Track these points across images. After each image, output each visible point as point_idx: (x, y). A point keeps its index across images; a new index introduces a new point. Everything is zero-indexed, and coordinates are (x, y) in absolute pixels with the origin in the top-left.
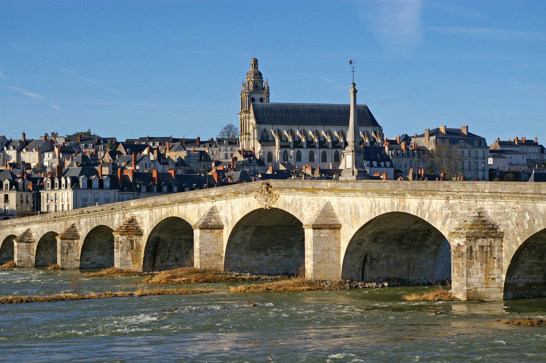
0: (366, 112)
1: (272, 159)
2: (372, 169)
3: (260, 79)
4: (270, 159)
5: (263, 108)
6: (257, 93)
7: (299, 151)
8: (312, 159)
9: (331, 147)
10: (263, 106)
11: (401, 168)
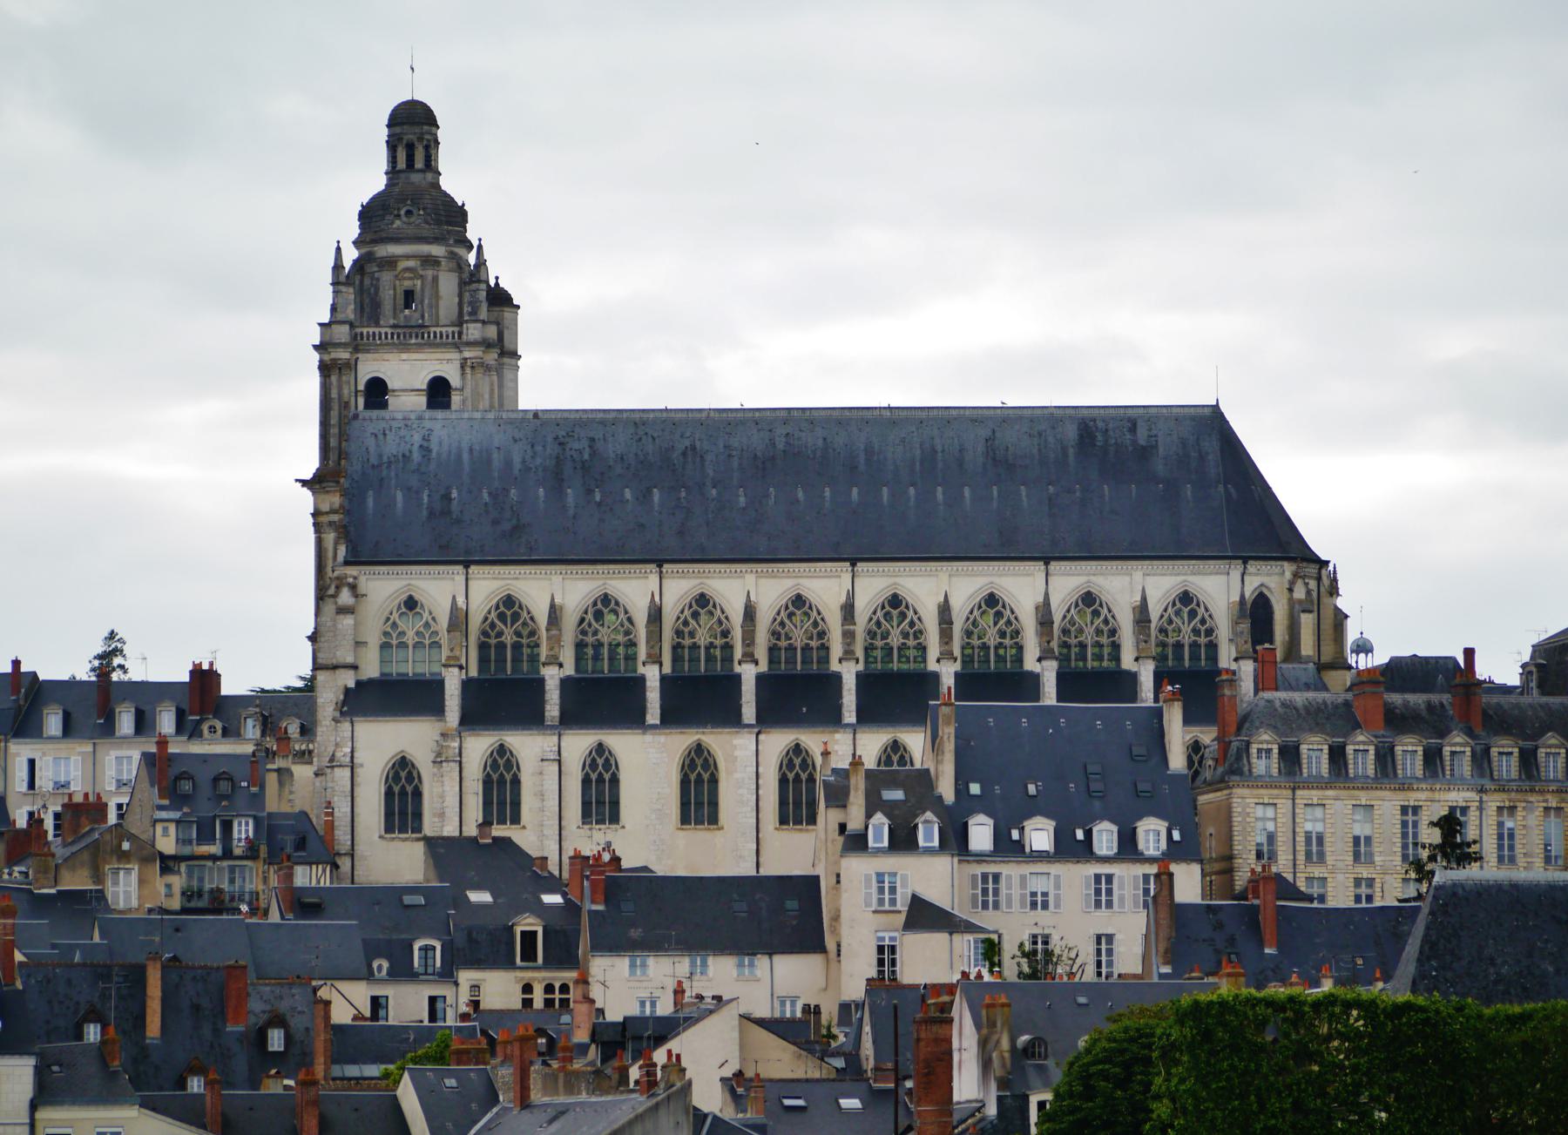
0: (1202, 458)
1: (418, 815)
2: (1011, 871)
3: (437, 250)
4: (403, 813)
5: (425, 450)
6: (404, 347)
7: (600, 748)
8: (699, 804)
9: (850, 716)
10: (426, 439)
11: (1321, 856)
